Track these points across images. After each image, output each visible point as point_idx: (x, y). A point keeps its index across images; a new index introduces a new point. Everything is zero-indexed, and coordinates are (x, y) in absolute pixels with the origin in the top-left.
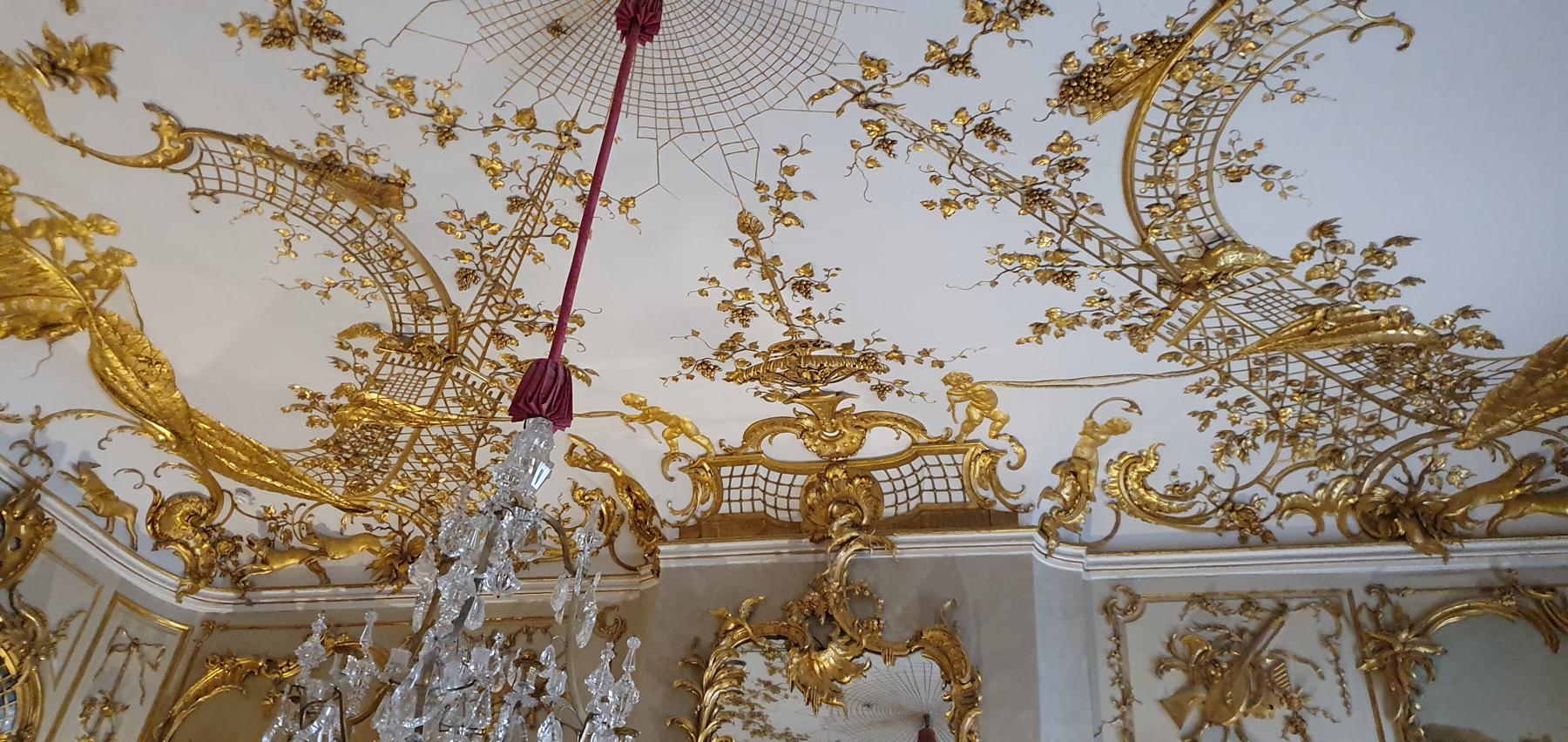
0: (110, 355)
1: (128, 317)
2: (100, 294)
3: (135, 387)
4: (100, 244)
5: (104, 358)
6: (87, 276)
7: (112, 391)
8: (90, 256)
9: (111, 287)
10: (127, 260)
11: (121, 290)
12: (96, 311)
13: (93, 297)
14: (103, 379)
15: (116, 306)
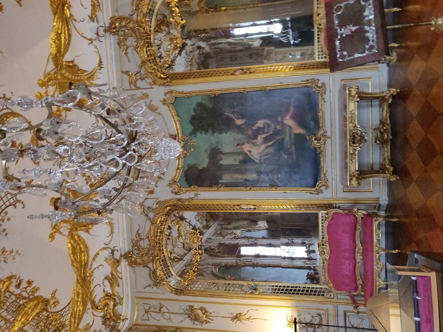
0: (62, 50)
1: (51, 60)
2: (53, 73)
3: (63, 34)
4: (43, 90)
5: (65, 49)
6: (52, 80)
7: (69, 36)
8: (48, 86)
9: (49, 74)
10: (41, 82)
11: (48, 71)
12: (57, 67)
13: (55, 73)
14: (69, 44)
15: (51, 66)
